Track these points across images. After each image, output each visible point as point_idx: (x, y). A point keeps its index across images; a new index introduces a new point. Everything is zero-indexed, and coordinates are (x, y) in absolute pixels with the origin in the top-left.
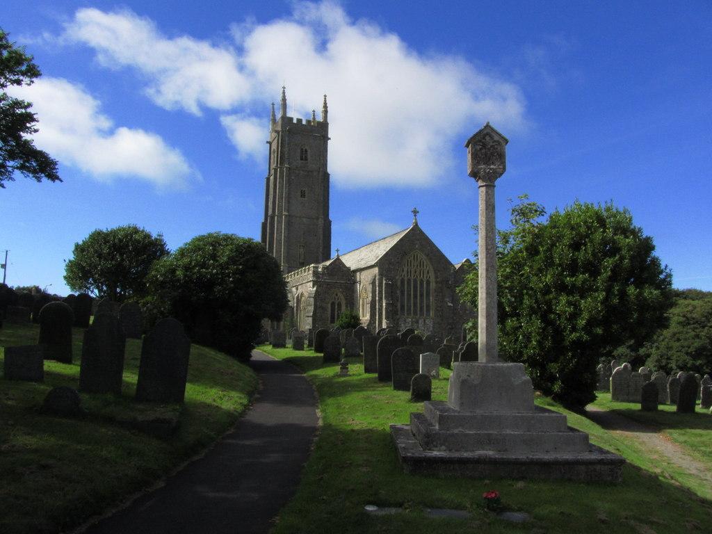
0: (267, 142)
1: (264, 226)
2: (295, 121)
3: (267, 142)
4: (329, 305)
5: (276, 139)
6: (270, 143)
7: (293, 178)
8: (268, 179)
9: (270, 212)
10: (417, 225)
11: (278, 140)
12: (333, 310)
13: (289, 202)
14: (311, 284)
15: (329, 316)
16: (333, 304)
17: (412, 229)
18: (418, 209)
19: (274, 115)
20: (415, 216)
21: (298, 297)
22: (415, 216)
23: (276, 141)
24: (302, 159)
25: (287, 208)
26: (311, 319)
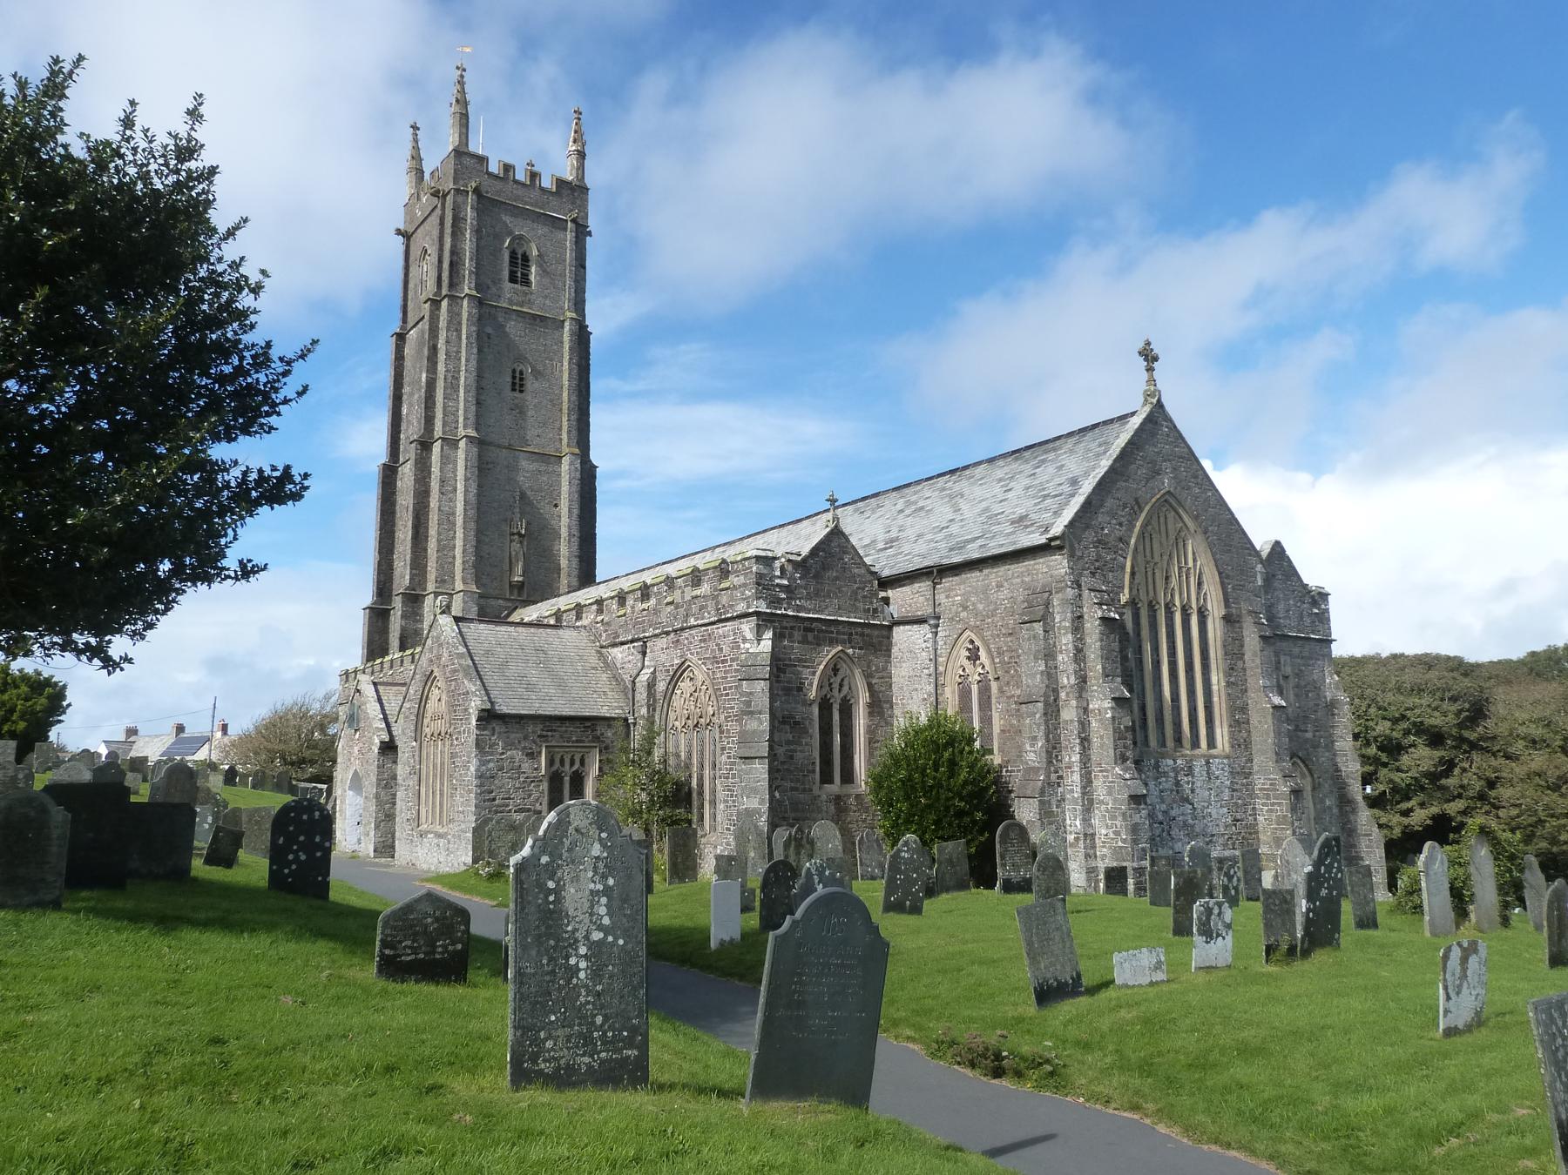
0: (399, 232)
1: (389, 473)
2: (494, 168)
3: (399, 232)
4: (816, 710)
5: (438, 211)
6: (407, 236)
7: (489, 330)
8: (401, 338)
9: (412, 429)
10: (1160, 405)
11: (442, 223)
12: (826, 731)
13: (478, 403)
14: (747, 628)
15: (816, 754)
16: (825, 706)
17: (1149, 419)
18: (1157, 349)
19: (417, 158)
20: (1150, 369)
21: (651, 685)
22: (1150, 369)
23: (435, 219)
24: (513, 279)
25: (472, 416)
26: (761, 770)
